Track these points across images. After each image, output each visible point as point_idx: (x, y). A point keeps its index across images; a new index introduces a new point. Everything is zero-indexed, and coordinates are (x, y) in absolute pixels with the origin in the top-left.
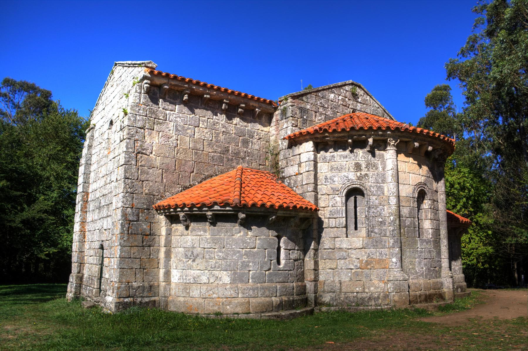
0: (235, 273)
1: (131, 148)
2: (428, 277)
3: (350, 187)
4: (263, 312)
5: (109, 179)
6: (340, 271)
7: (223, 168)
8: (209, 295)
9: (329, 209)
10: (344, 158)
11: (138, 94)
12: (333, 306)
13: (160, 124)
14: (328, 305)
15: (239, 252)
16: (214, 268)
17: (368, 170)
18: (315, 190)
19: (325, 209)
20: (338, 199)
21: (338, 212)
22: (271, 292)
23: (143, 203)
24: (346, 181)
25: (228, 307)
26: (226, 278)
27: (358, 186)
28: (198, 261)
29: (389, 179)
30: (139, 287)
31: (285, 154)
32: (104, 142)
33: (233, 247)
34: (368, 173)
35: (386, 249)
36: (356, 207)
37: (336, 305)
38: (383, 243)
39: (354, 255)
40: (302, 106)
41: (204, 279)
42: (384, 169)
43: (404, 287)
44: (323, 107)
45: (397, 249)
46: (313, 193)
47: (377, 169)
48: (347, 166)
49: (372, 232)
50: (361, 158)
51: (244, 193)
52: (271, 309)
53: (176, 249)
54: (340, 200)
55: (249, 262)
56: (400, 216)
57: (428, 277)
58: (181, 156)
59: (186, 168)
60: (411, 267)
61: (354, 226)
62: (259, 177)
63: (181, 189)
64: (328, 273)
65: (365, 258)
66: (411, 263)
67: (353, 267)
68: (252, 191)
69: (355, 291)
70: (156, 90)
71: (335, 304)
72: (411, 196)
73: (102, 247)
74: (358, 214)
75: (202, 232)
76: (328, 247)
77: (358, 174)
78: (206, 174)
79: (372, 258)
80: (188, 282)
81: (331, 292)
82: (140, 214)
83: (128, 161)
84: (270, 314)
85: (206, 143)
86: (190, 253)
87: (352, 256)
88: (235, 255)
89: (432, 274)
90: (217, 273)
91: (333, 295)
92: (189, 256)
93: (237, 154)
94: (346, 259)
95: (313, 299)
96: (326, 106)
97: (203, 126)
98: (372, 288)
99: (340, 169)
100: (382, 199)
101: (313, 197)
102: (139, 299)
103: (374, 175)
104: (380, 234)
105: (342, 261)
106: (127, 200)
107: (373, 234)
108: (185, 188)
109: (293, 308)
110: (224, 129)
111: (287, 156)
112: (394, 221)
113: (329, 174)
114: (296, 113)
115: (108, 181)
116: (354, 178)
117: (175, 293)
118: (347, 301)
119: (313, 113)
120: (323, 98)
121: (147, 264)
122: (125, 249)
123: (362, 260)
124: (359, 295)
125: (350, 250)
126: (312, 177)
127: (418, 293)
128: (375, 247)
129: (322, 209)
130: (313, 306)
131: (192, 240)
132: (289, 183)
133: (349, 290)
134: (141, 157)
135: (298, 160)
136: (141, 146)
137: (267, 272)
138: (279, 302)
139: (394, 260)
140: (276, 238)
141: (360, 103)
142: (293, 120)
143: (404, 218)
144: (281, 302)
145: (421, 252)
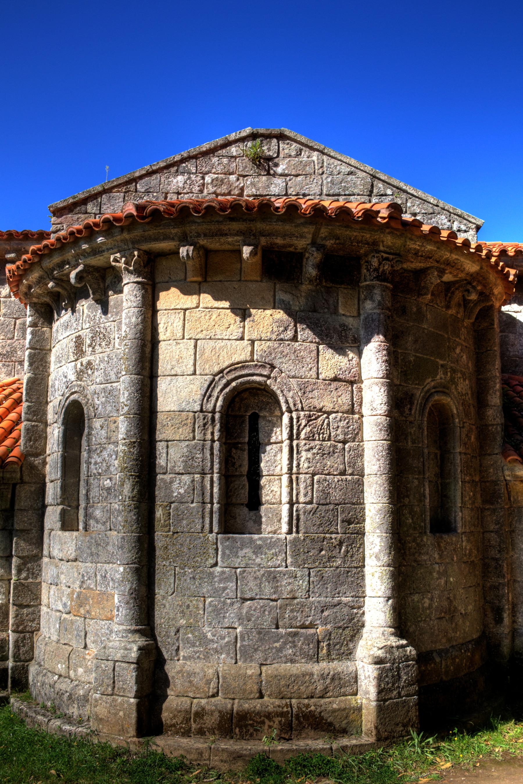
60: (183, 622)
104: (104, 523)
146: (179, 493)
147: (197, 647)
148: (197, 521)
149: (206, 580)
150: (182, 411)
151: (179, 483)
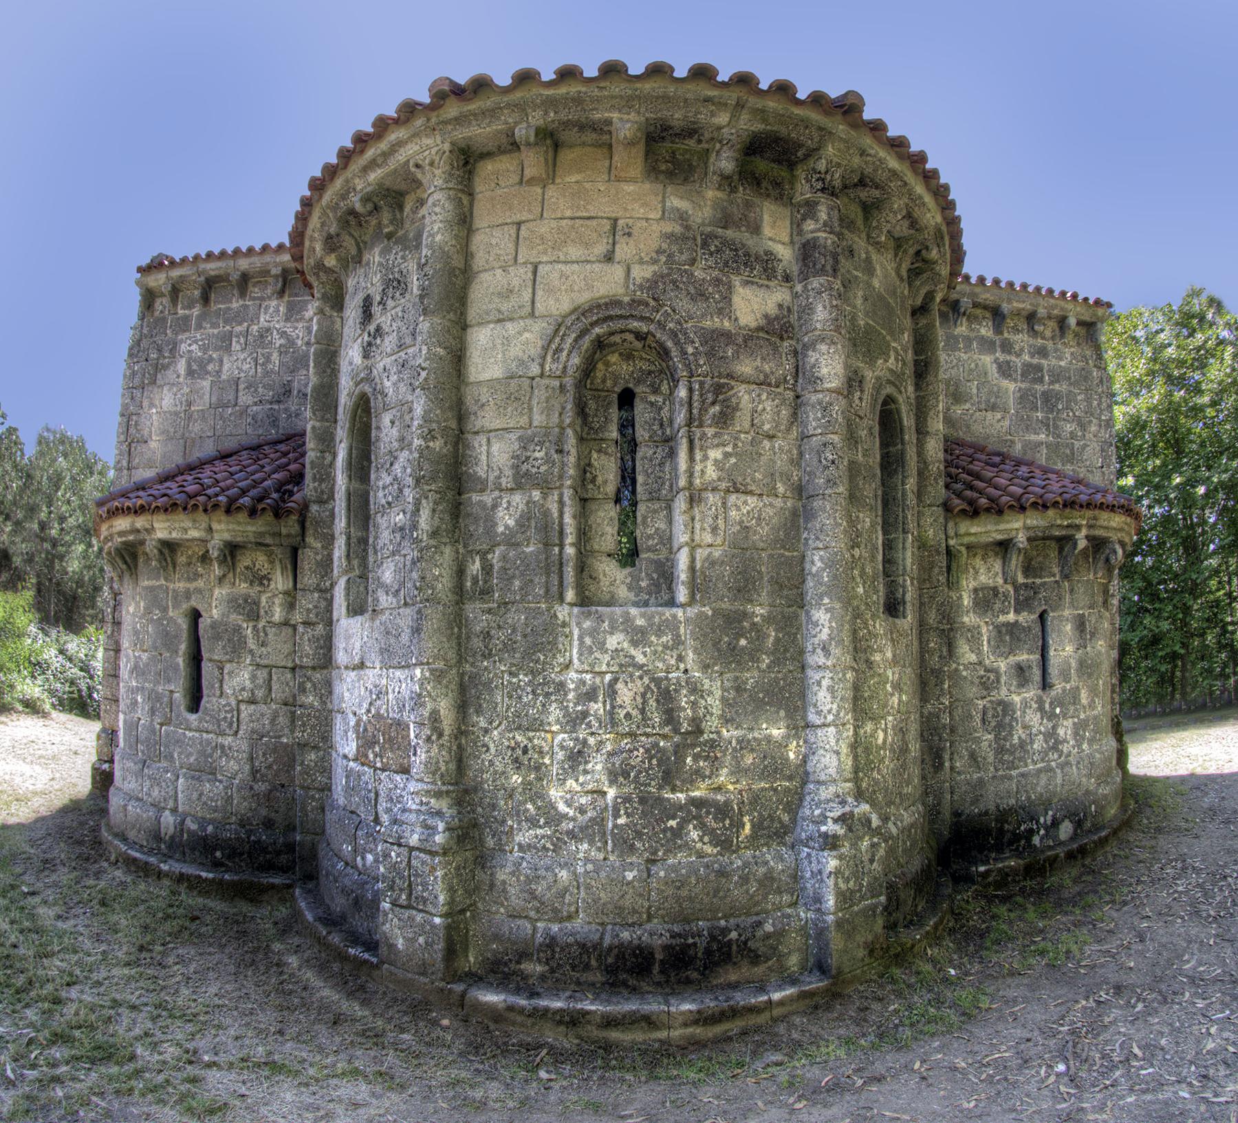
66: (520, 758)
110: (282, 341)
143: (487, 499)
146: (507, 527)
147: (540, 827)
148: (537, 580)
149: (553, 698)
150: (512, 378)
151: (507, 508)
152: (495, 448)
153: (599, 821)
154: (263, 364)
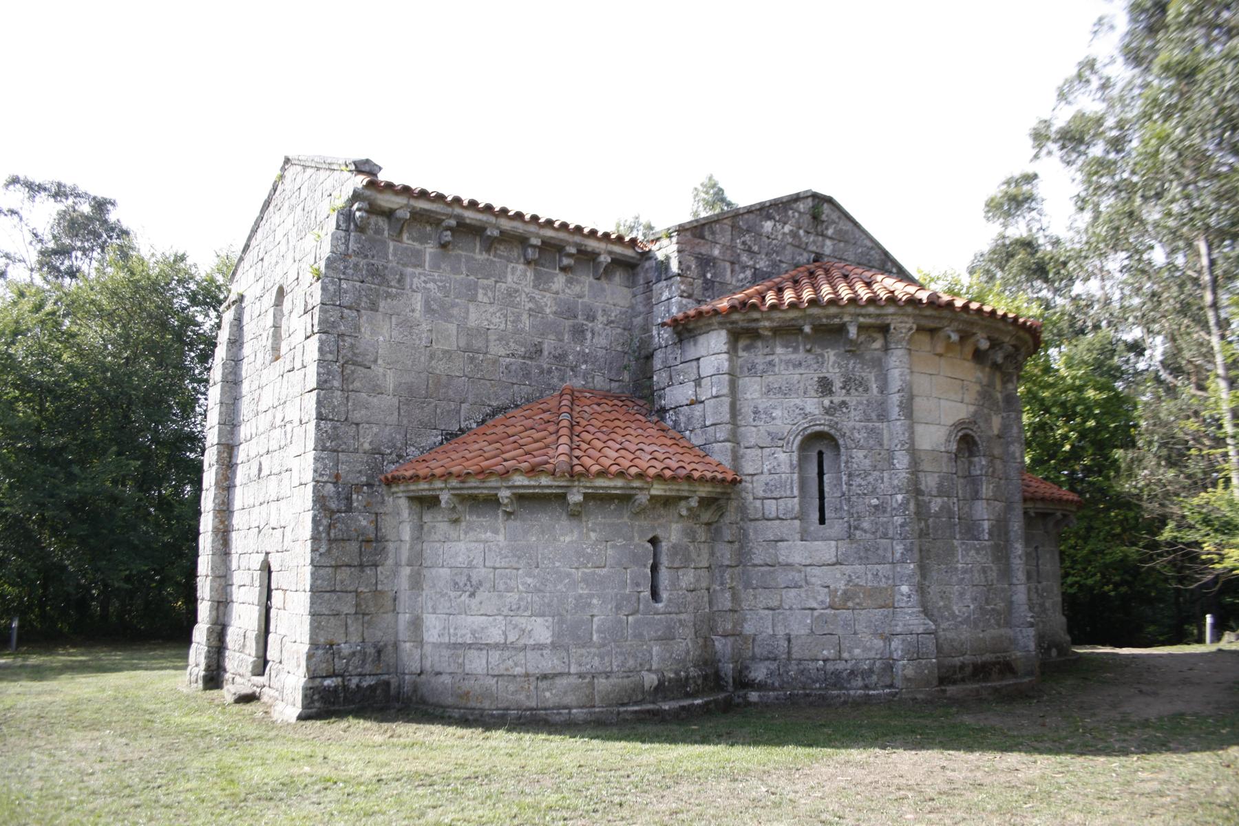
0: (562, 621)
1: (331, 352)
2: (981, 625)
3: (809, 431)
4: (623, 705)
5: (279, 417)
6: (788, 612)
7: (530, 390)
8: (507, 669)
9: (762, 478)
10: (795, 366)
11: (343, 234)
12: (774, 689)
13: (393, 297)
14: (760, 687)
15: (569, 575)
16: (516, 610)
17: (848, 392)
18: (734, 438)
19: (755, 478)
20: (782, 456)
21: (782, 485)
22: (639, 660)
23: (360, 472)
24: (800, 418)
25: (548, 694)
26: (542, 631)
27: (826, 429)
28: (482, 595)
29: (895, 412)
30: (354, 654)
31: (666, 358)
32: (265, 336)
33: (557, 564)
34: (847, 399)
35: (888, 566)
36: (821, 474)
37: (782, 688)
38: (880, 552)
39: (818, 576)
40: (703, 251)
41: (495, 636)
42: (883, 389)
43: (927, 648)
44: (749, 250)
45: (912, 566)
46: (728, 445)
47: (866, 390)
48: (802, 384)
49: (856, 528)
50: (833, 366)
51: (578, 447)
52: (640, 697)
53: (434, 571)
54: (785, 458)
55: (591, 596)
56: (918, 492)
57: (981, 625)
58: (441, 367)
59: (451, 393)
60: (941, 604)
61: (815, 516)
62: (609, 409)
63: (440, 438)
64: (761, 618)
65: (842, 586)
66: (943, 595)
67: (815, 605)
68: (595, 442)
69: (820, 657)
70: (381, 223)
71: (777, 684)
72: (943, 449)
73: (267, 569)
74: (826, 489)
75: (489, 534)
76: (761, 562)
77: (827, 402)
78: (494, 404)
79: (857, 585)
80: (460, 641)
81: (768, 659)
82: (354, 496)
83: (326, 381)
84: (636, 708)
85: (492, 337)
86: (464, 579)
87: (813, 580)
88: (561, 582)
89: (989, 620)
90: (523, 620)
91: (774, 666)
92: (461, 584)
93: (560, 357)
94: (801, 587)
95: (730, 673)
96: (756, 248)
97: (486, 300)
98: (857, 651)
99: (785, 392)
100: (878, 457)
101: (729, 453)
102: (355, 681)
103: (861, 403)
104: (873, 533)
105: (793, 592)
106: (325, 466)
107: (858, 533)
108: (450, 436)
109: (688, 695)
110: (531, 305)
111: (671, 362)
112: (905, 504)
113: (763, 404)
114: (689, 268)
115: (278, 422)
116: (817, 412)
117: (432, 666)
118: (803, 679)
119: (728, 265)
120: (748, 231)
121: (371, 604)
122: (322, 572)
123: (836, 590)
124: (830, 667)
125: (809, 569)
126: (726, 409)
127: (957, 661)
128: (864, 560)
129: (748, 478)
130: (730, 689)
131: (469, 550)
132: (675, 422)
133: (807, 654)
134: (353, 372)
135: (695, 371)
136: (352, 346)
137: (630, 618)
138: (656, 682)
139: (905, 589)
140: (649, 545)
141: (831, 238)
142: (682, 282)
143: (927, 499)
144: (661, 684)
145: (965, 572)
152: (929, 479)
153: (969, 617)
154: (513, 322)
